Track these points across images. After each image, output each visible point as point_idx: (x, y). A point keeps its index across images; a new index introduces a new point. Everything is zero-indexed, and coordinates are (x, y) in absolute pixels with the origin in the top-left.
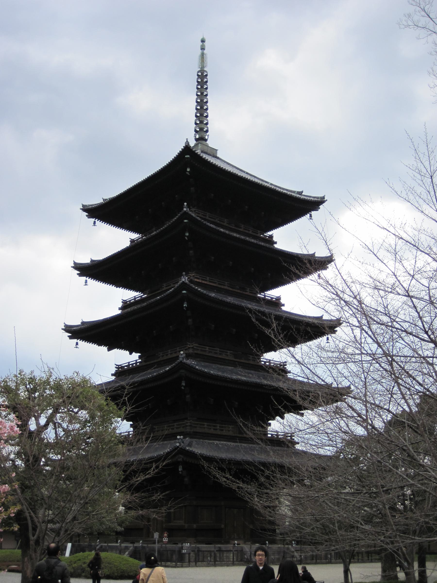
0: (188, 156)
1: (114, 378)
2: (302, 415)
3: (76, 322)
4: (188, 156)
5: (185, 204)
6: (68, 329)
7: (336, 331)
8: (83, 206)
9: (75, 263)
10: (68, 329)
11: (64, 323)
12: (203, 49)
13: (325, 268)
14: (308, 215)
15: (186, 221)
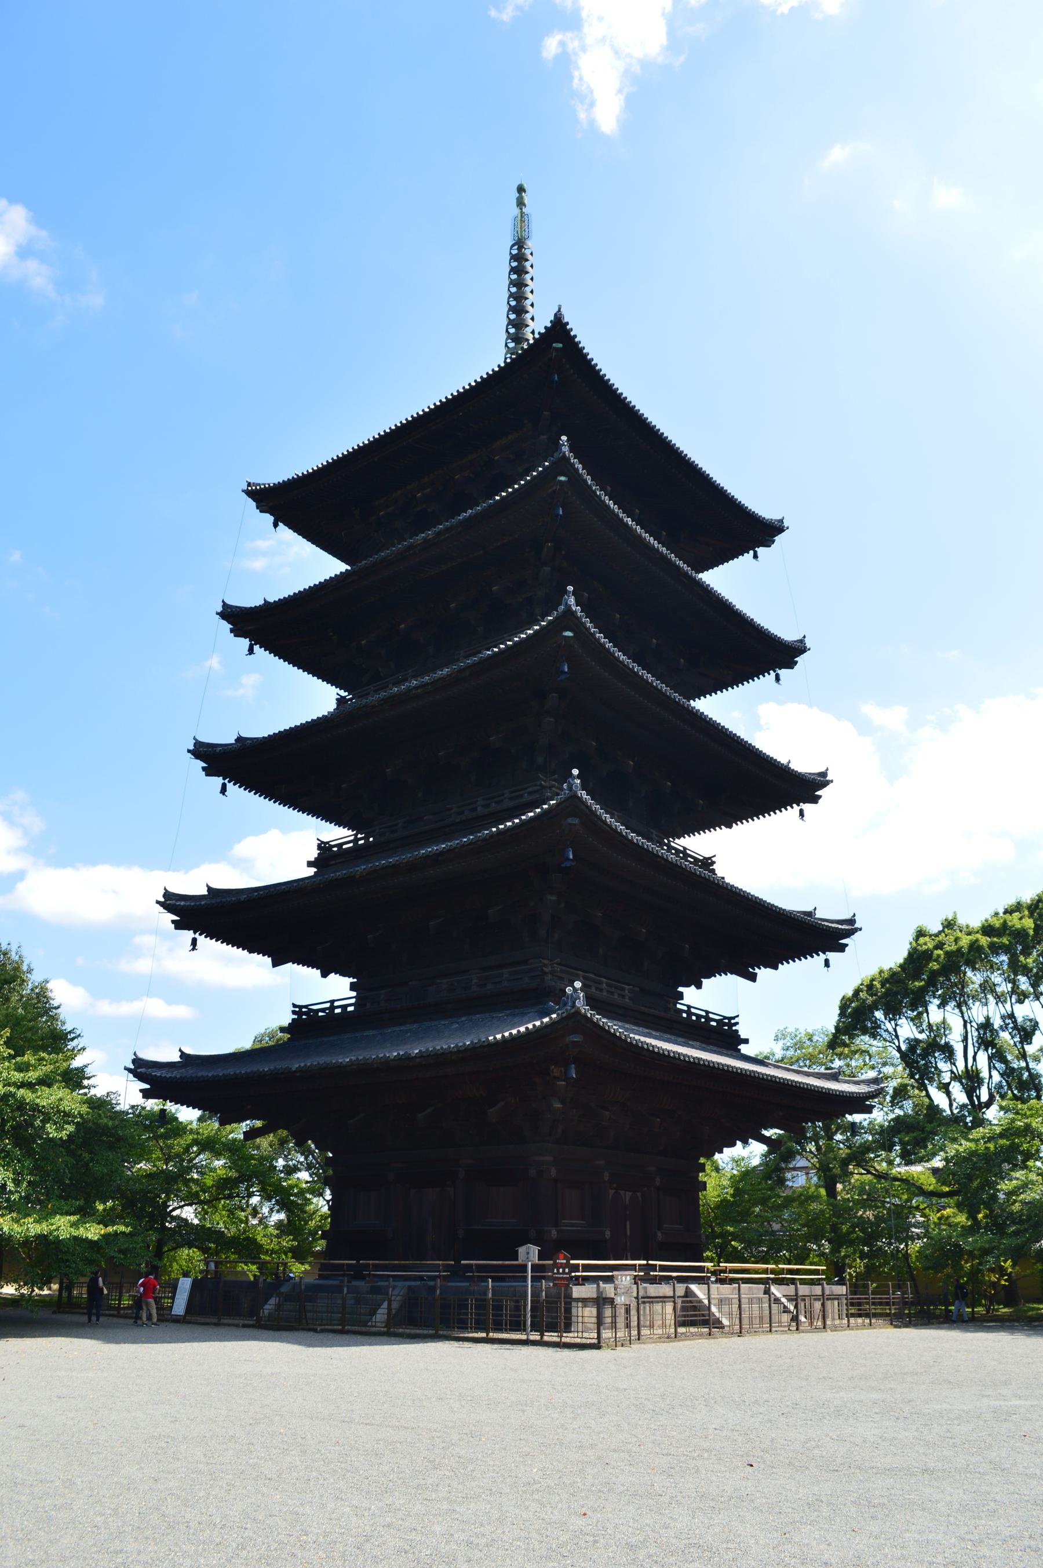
0: (561, 345)
1: (311, 871)
2: (753, 978)
3: (222, 734)
4: (561, 345)
5: (564, 438)
6: (202, 751)
7: (820, 797)
8: (249, 484)
9: (225, 604)
10: (202, 751)
11: (194, 738)
12: (521, 203)
13: (791, 664)
14: (752, 552)
15: (563, 478)
